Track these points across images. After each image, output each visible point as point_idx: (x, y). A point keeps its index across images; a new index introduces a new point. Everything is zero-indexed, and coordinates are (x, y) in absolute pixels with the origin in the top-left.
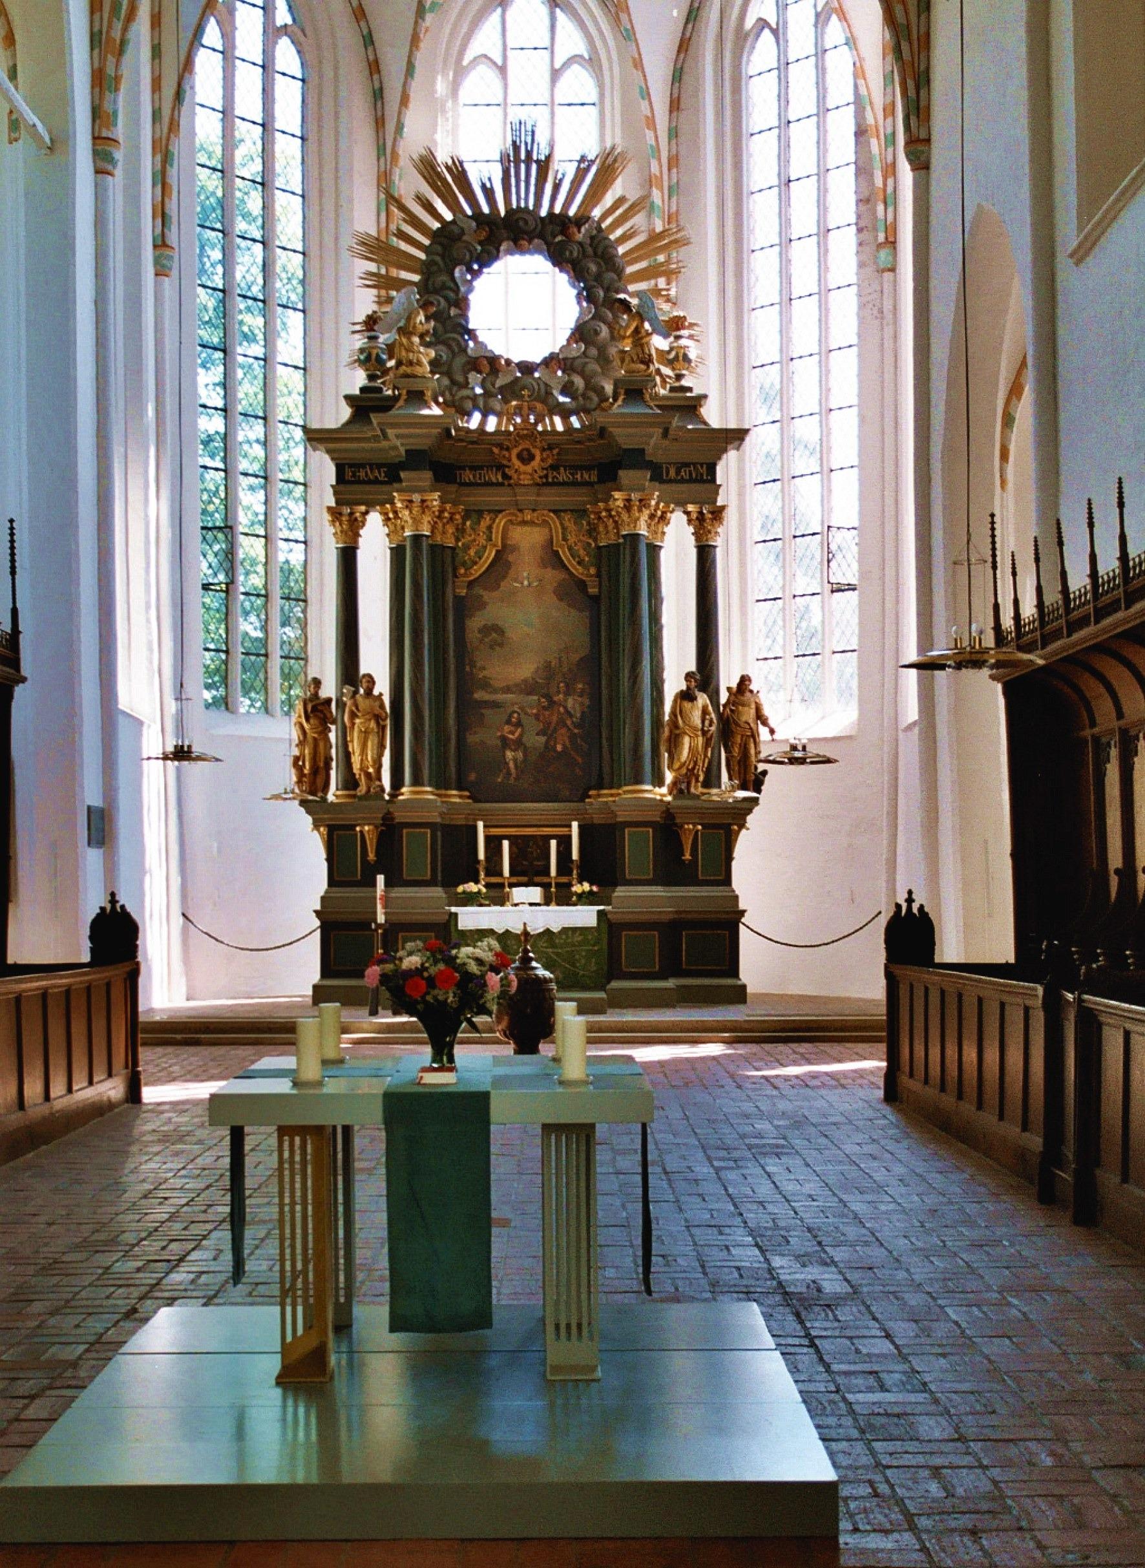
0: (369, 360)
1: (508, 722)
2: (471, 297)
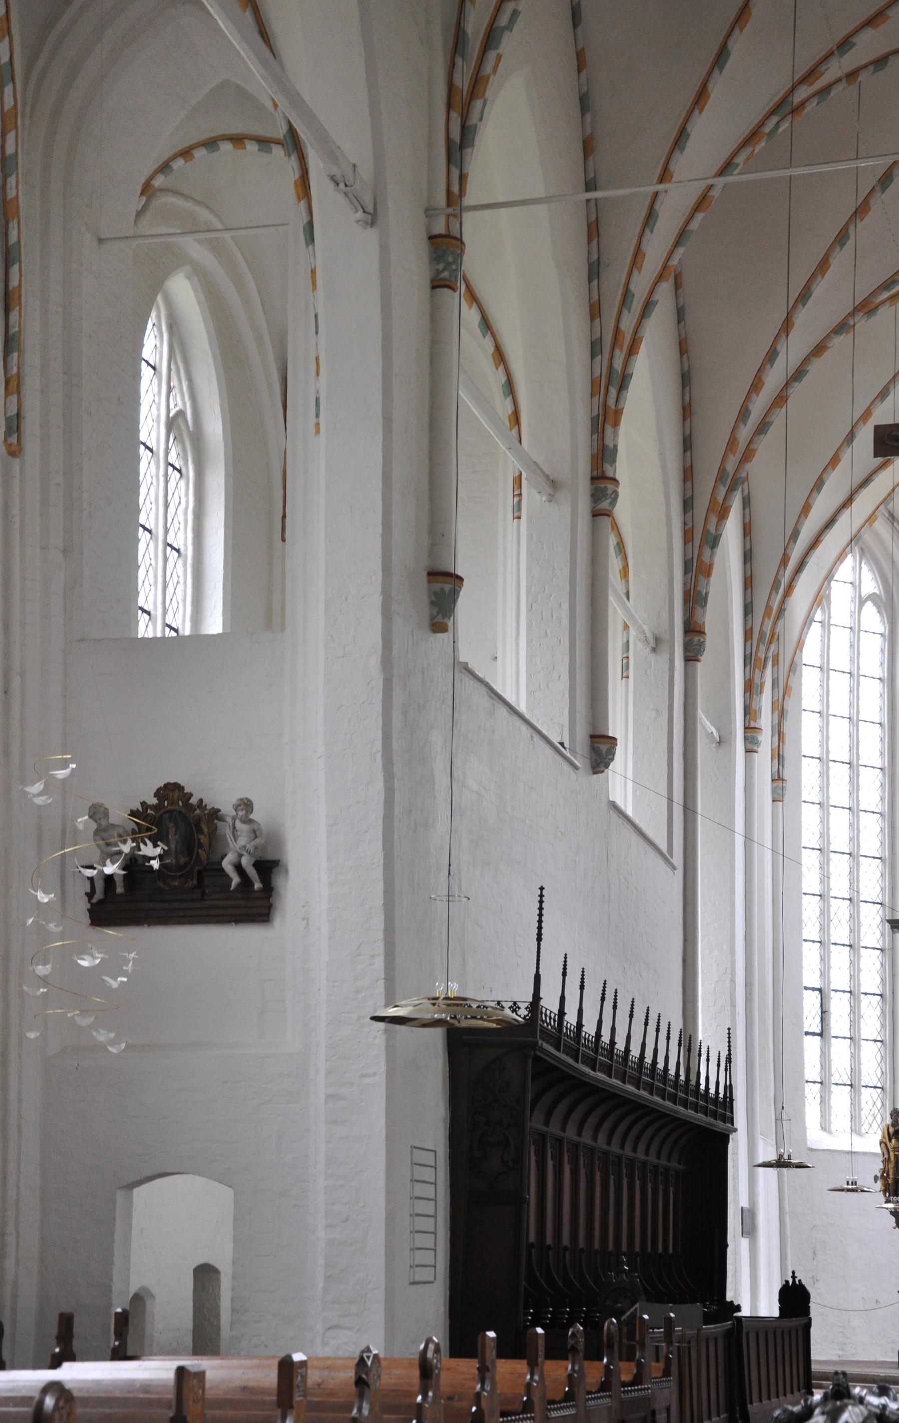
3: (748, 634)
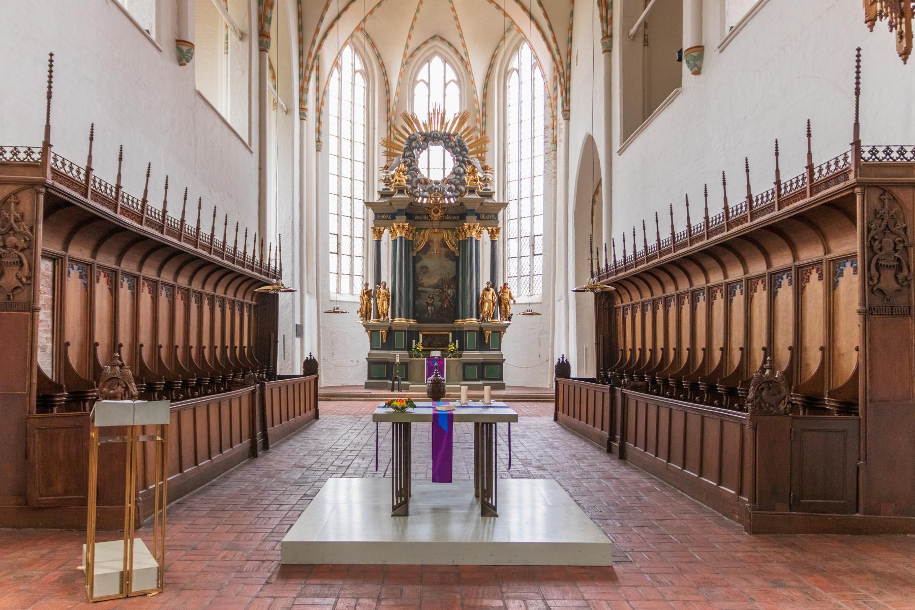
0: (387, 181)
1: (429, 297)
2: (419, 159)
3: (301, 65)
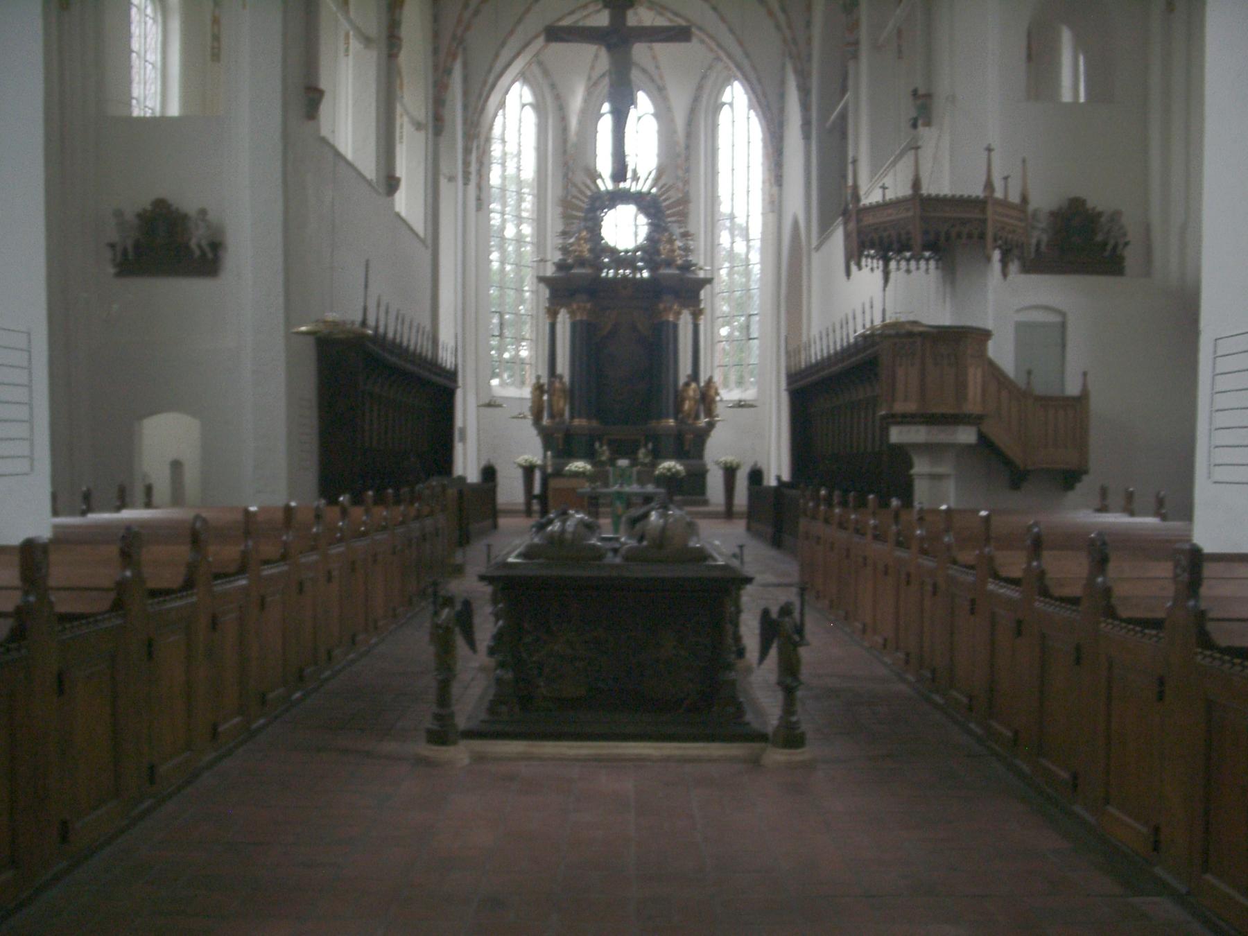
0: (565, 250)
